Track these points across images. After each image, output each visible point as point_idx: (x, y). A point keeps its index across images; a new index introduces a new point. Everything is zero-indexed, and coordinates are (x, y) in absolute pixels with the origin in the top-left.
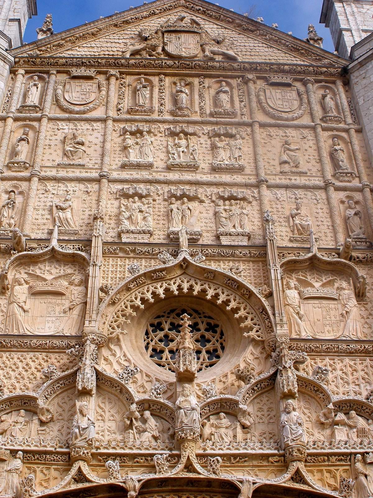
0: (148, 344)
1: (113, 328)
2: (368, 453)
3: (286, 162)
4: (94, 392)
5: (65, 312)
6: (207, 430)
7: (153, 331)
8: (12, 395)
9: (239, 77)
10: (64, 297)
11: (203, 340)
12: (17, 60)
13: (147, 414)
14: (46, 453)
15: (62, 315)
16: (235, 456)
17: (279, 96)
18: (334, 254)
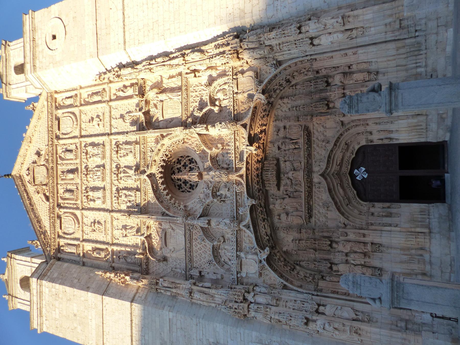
0: (187, 191)
2: (233, 91)
3: (99, 125)
4: (209, 219)
5: (174, 231)
6: (225, 166)
7: (182, 189)
9: (56, 147)
10: (167, 232)
11: (185, 166)
12: (53, 258)
14: (237, 241)
15: (175, 232)
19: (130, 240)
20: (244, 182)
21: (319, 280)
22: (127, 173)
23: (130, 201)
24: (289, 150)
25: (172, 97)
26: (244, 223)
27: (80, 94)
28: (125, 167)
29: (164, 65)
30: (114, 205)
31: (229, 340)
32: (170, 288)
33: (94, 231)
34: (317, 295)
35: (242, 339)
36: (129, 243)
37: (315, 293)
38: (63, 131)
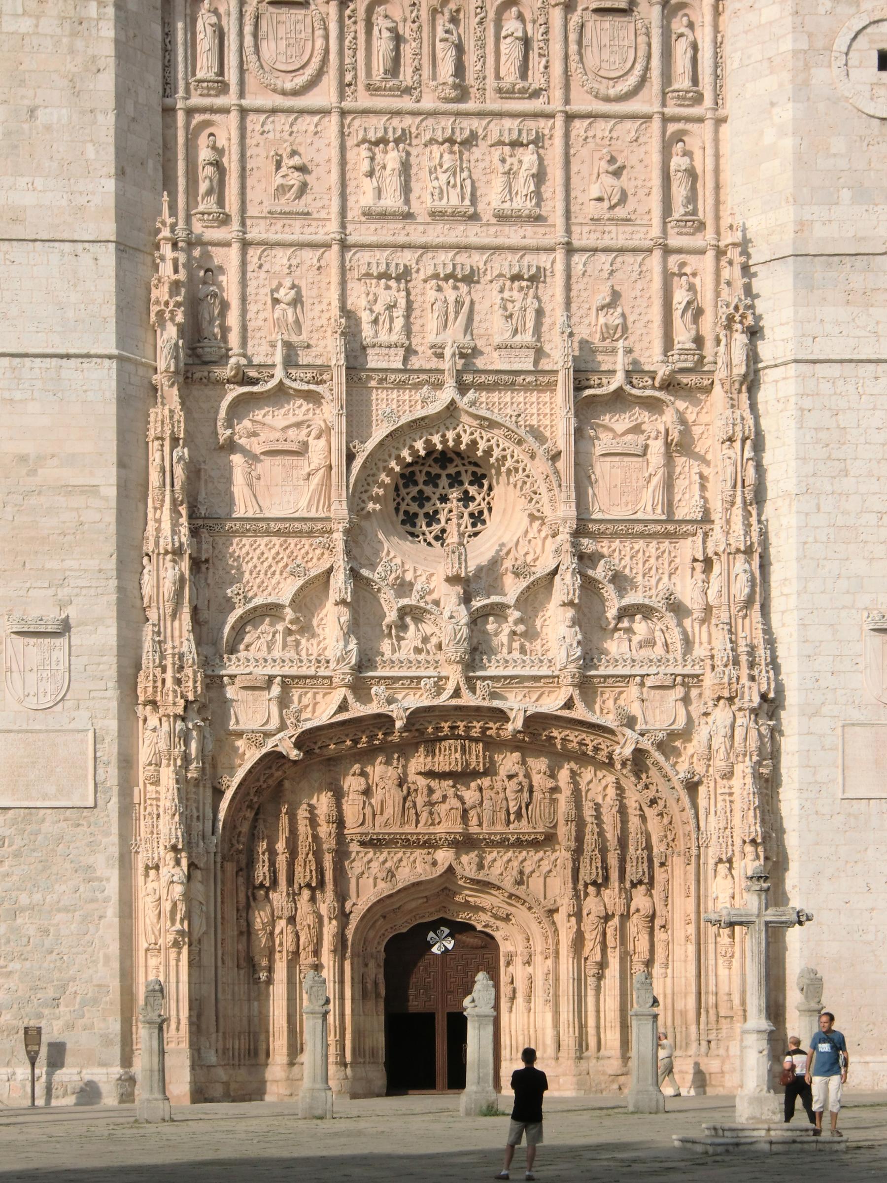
1: (363, 502)
3: (600, 199)
8: (258, 601)
13: (408, 620)
14: (306, 677)
15: (302, 483)
16: (505, 678)
17: (605, 40)
18: (646, 379)
19: (262, 316)
20: (443, 699)
21: (238, 862)
22: (457, 313)
23: (375, 321)
24: (506, 799)
25: (651, 489)
26: (351, 699)
27: (700, 120)
28: (472, 303)
29: (735, 486)
30: (365, 256)
31: (84, 660)
32: (172, 485)
33: (278, 166)
34: (215, 862)
35: (93, 694)
36: (252, 308)
37: (219, 860)
38: (592, 22)
